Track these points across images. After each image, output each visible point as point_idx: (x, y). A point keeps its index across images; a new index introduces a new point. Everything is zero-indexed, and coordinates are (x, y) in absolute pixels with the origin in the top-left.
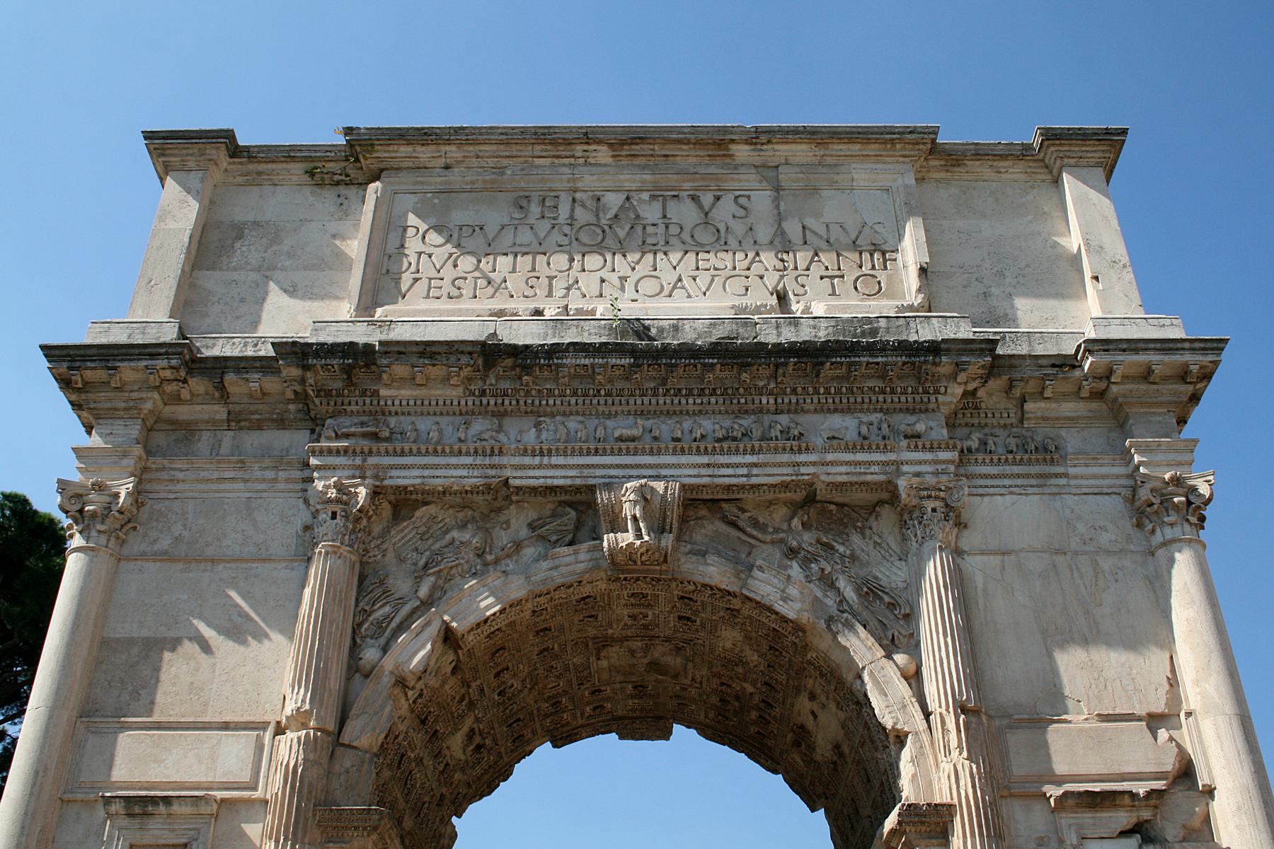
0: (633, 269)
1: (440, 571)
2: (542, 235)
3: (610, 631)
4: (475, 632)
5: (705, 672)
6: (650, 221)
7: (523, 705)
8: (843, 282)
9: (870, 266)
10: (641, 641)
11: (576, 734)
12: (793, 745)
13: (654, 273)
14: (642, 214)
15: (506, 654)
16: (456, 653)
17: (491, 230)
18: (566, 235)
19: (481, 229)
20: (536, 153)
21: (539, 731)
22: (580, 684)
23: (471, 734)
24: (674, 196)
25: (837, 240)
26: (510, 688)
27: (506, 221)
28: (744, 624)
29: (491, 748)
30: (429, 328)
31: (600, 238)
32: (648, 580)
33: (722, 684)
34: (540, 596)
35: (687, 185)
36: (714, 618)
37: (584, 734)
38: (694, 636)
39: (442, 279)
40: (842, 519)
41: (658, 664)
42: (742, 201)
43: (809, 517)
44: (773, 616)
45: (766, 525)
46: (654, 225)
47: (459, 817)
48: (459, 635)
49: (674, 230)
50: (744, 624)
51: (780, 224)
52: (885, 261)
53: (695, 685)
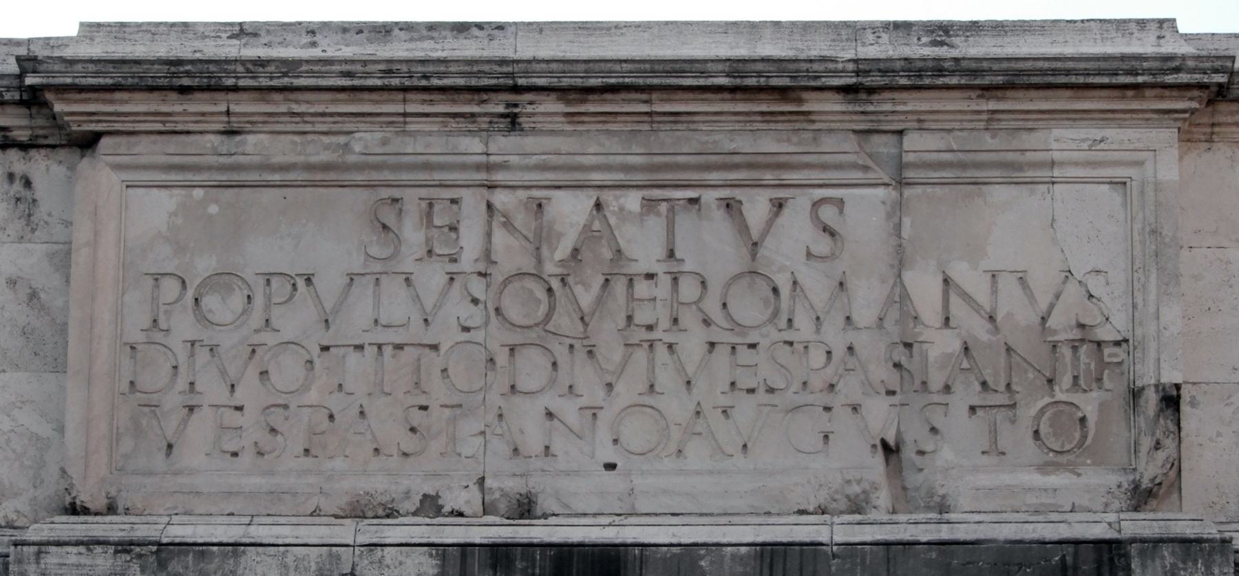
0: (610, 386)
2: (429, 304)
6: (643, 267)
8: (1013, 421)
9: (1067, 381)
13: (648, 400)
14: (629, 250)
17: (329, 284)
18: (475, 301)
19: (309, 281)
20: (411, 108)
24: (694, 201)
25: (1009, 315)
27: (357, 265)
30: (231, 561)
31: (543, 309)
35: (714, 177)
39: (239, 408)
42: (828, 214)
46: (650, 276)
49: (689, 290)
51: (900, 276)
52: (1102, 365)
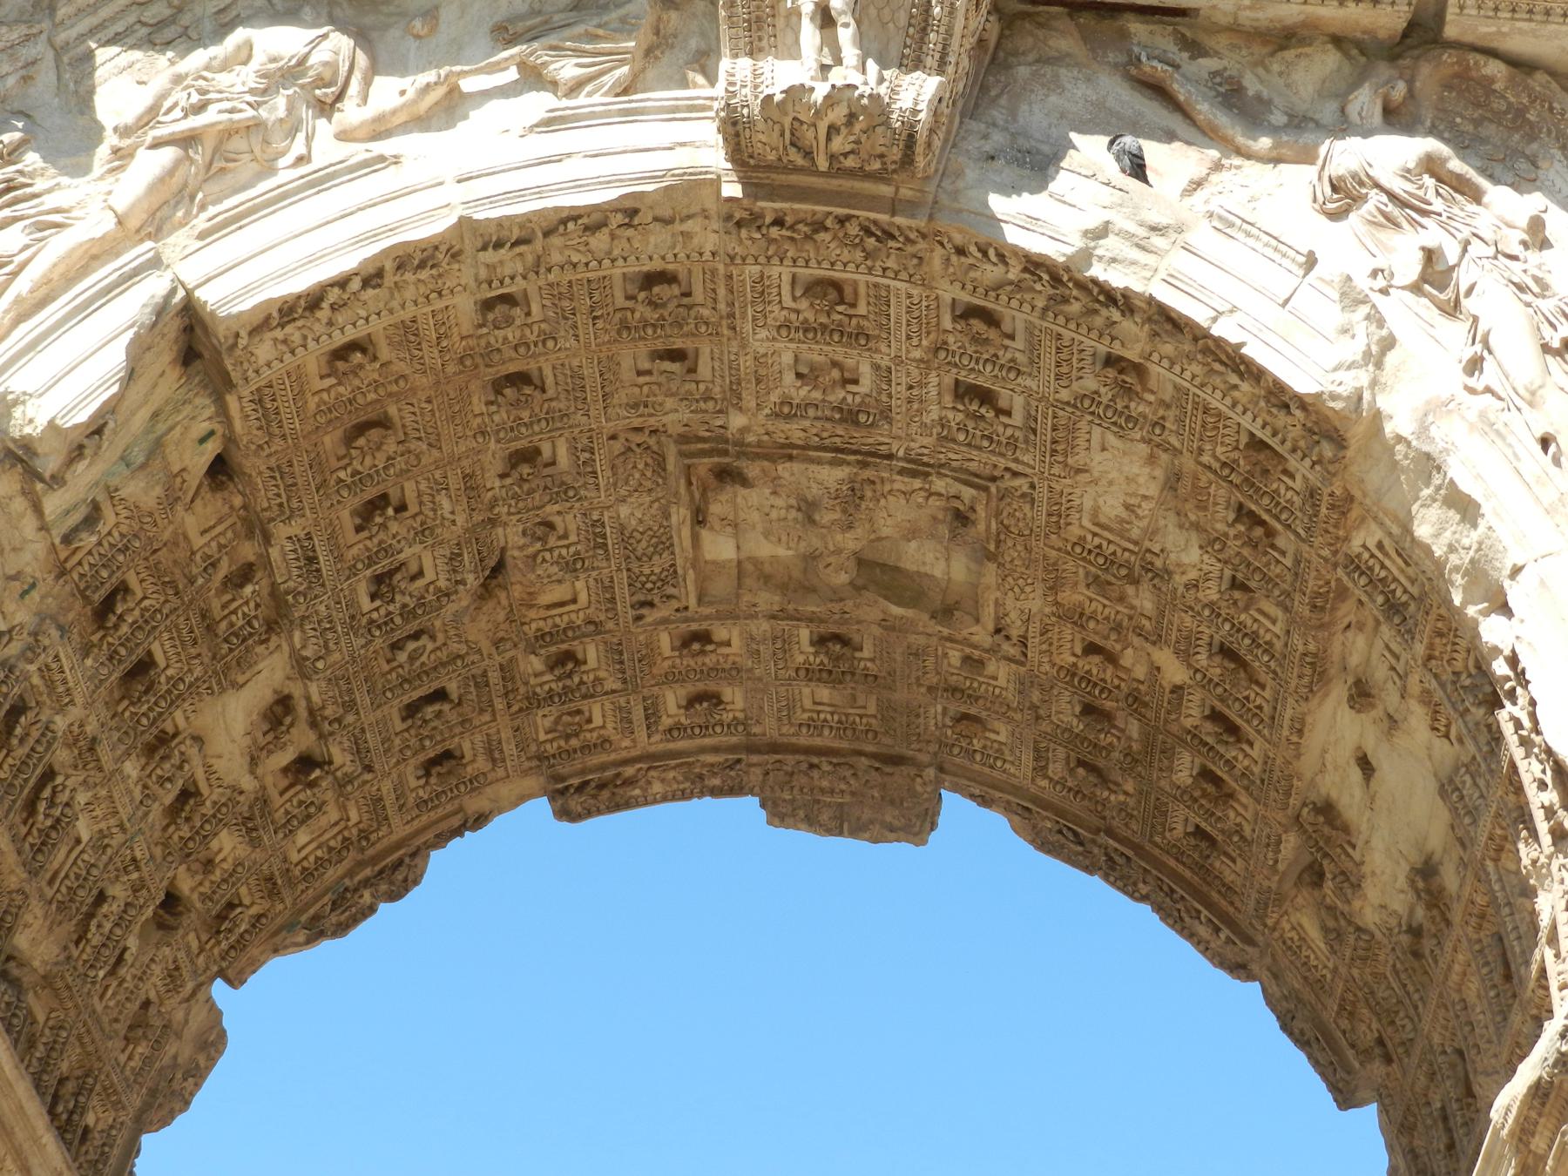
1: (187, 141)
3: (737, 421)
4: (279, 334)
5: (1036, 602)
7: (456, 647)
10: (834, 463)
11: (630, 782)
12: (1299, 882)
15: (391, 447)
16: (221, 402)
21: (510, 748)
22: (643, 604)
23: (279, 710)
26: (413, 578)
28: (1159, 424)
29: (349, 779)
32: (853, 229)
33: (1091, 649)
34: (498, 245)
36: (1065, 395)
37: (657, 788)
38: (1002, 463)
40: (1521, 113)
41: (897, 569)
43: (1411, 94)
44: (1245, 386)
45: (1265, 104)
47: (235, 981)
48: (221, 331)
50: (1159, 424)
53: (1006, 646)
